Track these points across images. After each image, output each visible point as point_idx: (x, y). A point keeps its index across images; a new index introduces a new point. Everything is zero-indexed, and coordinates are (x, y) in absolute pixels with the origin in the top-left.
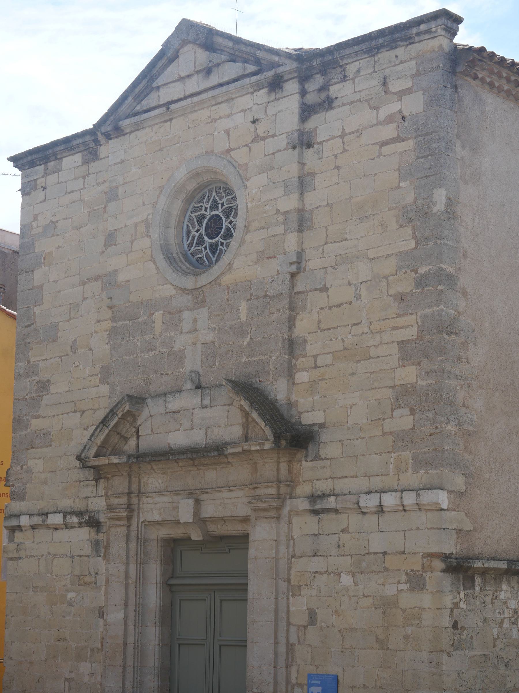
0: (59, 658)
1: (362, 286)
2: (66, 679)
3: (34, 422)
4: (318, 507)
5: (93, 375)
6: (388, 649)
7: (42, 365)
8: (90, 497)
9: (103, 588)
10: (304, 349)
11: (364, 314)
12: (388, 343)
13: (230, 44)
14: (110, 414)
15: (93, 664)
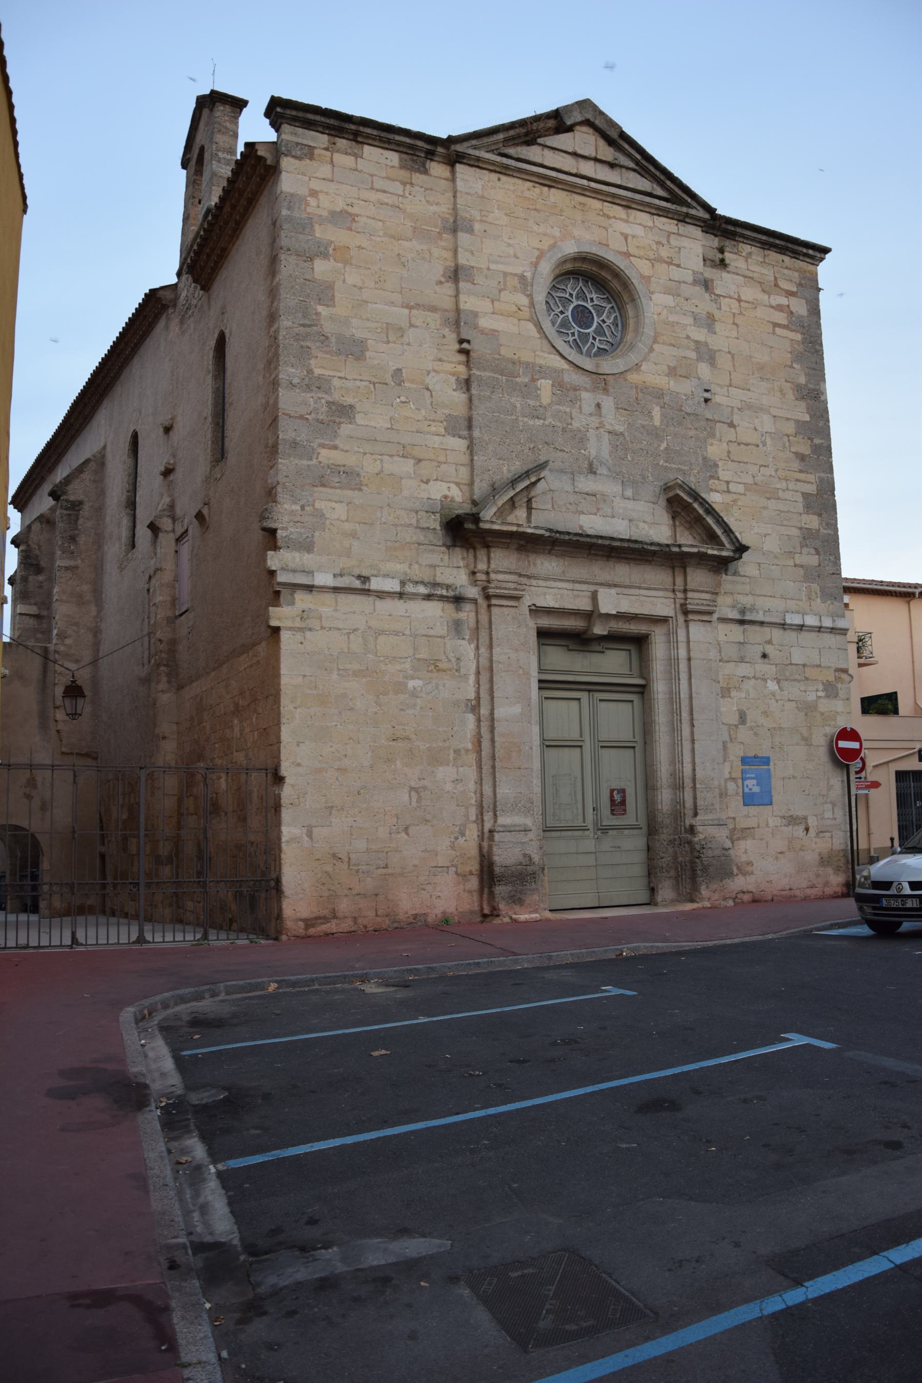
0: (398, 763)
1: (767, 435)
2: (412, 789)
3: (324, 452)
4: (747, 617)
5: (434, 421)
6: (811, 745)
7: (336, 383)
8: (438, 566)
9: (472, 679)
10: (716, 472)
11: (771, 459)
12: (793, 490)
13: (639, 157)
14: (524, 475)
15: (461, 769)
